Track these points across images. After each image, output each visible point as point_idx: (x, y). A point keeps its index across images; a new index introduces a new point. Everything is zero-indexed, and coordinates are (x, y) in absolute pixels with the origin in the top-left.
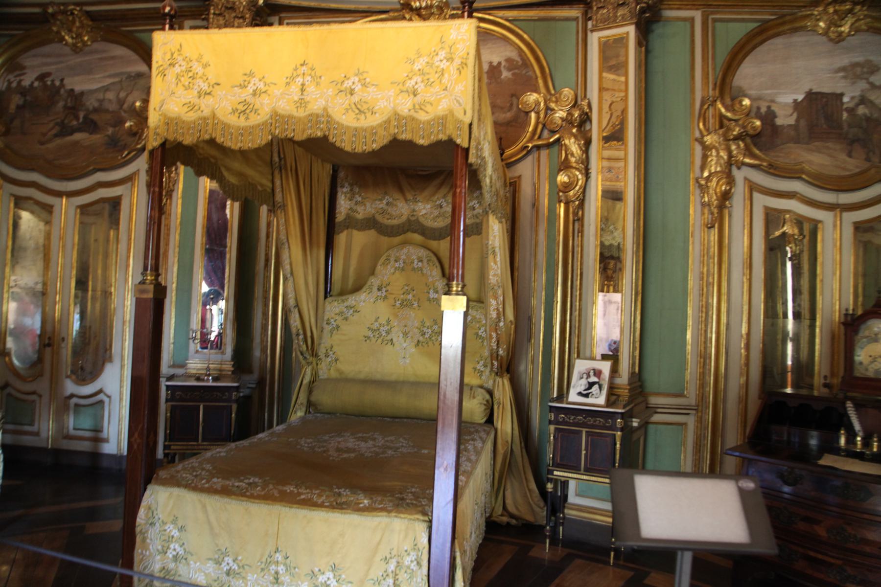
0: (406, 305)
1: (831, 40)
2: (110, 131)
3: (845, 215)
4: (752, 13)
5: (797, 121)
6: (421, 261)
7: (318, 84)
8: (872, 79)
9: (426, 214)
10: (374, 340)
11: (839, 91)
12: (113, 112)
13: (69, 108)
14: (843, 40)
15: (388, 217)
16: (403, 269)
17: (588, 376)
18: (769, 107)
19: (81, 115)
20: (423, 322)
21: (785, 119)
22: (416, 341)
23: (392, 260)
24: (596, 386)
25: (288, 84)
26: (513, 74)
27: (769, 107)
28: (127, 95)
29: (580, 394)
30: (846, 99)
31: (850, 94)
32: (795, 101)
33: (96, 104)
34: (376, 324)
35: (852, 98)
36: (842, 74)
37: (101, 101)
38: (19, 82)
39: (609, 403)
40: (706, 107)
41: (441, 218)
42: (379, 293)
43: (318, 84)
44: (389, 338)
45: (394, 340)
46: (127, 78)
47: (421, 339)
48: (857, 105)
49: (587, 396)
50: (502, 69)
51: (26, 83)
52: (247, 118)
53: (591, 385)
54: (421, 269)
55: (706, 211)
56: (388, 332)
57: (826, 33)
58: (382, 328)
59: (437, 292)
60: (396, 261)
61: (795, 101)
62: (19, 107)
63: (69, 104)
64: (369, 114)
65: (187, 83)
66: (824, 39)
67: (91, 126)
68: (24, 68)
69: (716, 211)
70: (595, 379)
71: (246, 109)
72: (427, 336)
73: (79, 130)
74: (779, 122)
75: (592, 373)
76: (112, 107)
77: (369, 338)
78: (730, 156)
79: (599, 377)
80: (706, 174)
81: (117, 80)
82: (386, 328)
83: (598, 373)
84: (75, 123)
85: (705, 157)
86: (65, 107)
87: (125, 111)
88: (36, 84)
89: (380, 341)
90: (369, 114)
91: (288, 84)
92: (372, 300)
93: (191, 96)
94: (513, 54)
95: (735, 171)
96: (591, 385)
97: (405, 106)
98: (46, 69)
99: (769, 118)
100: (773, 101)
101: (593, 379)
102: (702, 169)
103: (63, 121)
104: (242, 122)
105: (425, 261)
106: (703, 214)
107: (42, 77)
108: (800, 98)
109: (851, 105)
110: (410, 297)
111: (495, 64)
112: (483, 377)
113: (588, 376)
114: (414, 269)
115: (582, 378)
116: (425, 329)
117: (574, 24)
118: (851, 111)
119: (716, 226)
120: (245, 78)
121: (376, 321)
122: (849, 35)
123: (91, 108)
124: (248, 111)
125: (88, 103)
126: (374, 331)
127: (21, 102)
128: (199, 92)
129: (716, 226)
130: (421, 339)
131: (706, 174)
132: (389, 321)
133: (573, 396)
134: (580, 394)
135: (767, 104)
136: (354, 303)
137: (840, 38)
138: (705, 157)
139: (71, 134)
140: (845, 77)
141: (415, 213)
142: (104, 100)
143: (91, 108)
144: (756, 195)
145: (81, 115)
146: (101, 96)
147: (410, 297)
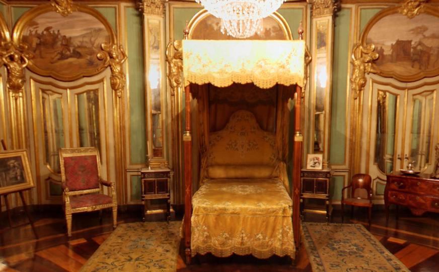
1: (408, 17)
2: (89, 57)
3: (410, 91)
5: (392, 53)
11: (410, 40)
12: (88, 48)
13: (64, 45)
14: (414, 17)
17: (314, 160)
18: (381, 48)
19: (72, 49)
21: (388, 52)
26: (276, 34)
27: (381, 48)
28: (95, 40)
29: (311, 166)
30: (413, 43)
31: (415, 40)
32: (392, 45)
33: (79, 44)
35: (416, 42)
36: (412, 32)
37: (82, 42)
38: (36, 31)
40: (355, 48)
44: (236, 147)
46: (94, 31)
48: (418, 45)
49: (314, 167)
50: (271, 32)
51: (40, 32)
53: (315, 163)
55: (353, 92)
56: (235, 146)
57: (406, 14)
60: (238, 117)
61: (392, 45)
62: (37, 45)
63: (64, 43)
66: (406, 17)
67: (77, 55)
68: (37, 24)
69: (358, 92)
70: (317, 161)
73: (71, 57)
74: (385, 53)
76: (89, 45)
78: (365, 69)
80: (354, 77)
81: (89, 31)
84: (68, 53)
85: (354, 70)
86: (62, 45)
87: (95, 48)
88: (45, 33)
94: (275, 25)
95: (366, 75)
98: (50, 25)
99: (381, 52)
100: (383, 45)
102: (352, 75)
103: (62, 52)
106: (352, 93)
107: (48, 29)
108: (394, 43)
109: (415, 46)
111: (268, 29)
117: (301, 11)
118: (415, 48)
119: (358, 98)
122: (416, 15)
123: (76, 46)
125: (74, 43)
127: (38, 42)
129: (358, 98)
130: (249, 147)
131: (354, 77)
134: (311, 166)
135: (380, 46)
137: (412, 16)
138: (354, 70)
139: (67, 58)
140: (413, 33)
142: (83, 42)
143: (76, 46)
144: (375, 84)
145: (72, 49)
146: (81, 39)
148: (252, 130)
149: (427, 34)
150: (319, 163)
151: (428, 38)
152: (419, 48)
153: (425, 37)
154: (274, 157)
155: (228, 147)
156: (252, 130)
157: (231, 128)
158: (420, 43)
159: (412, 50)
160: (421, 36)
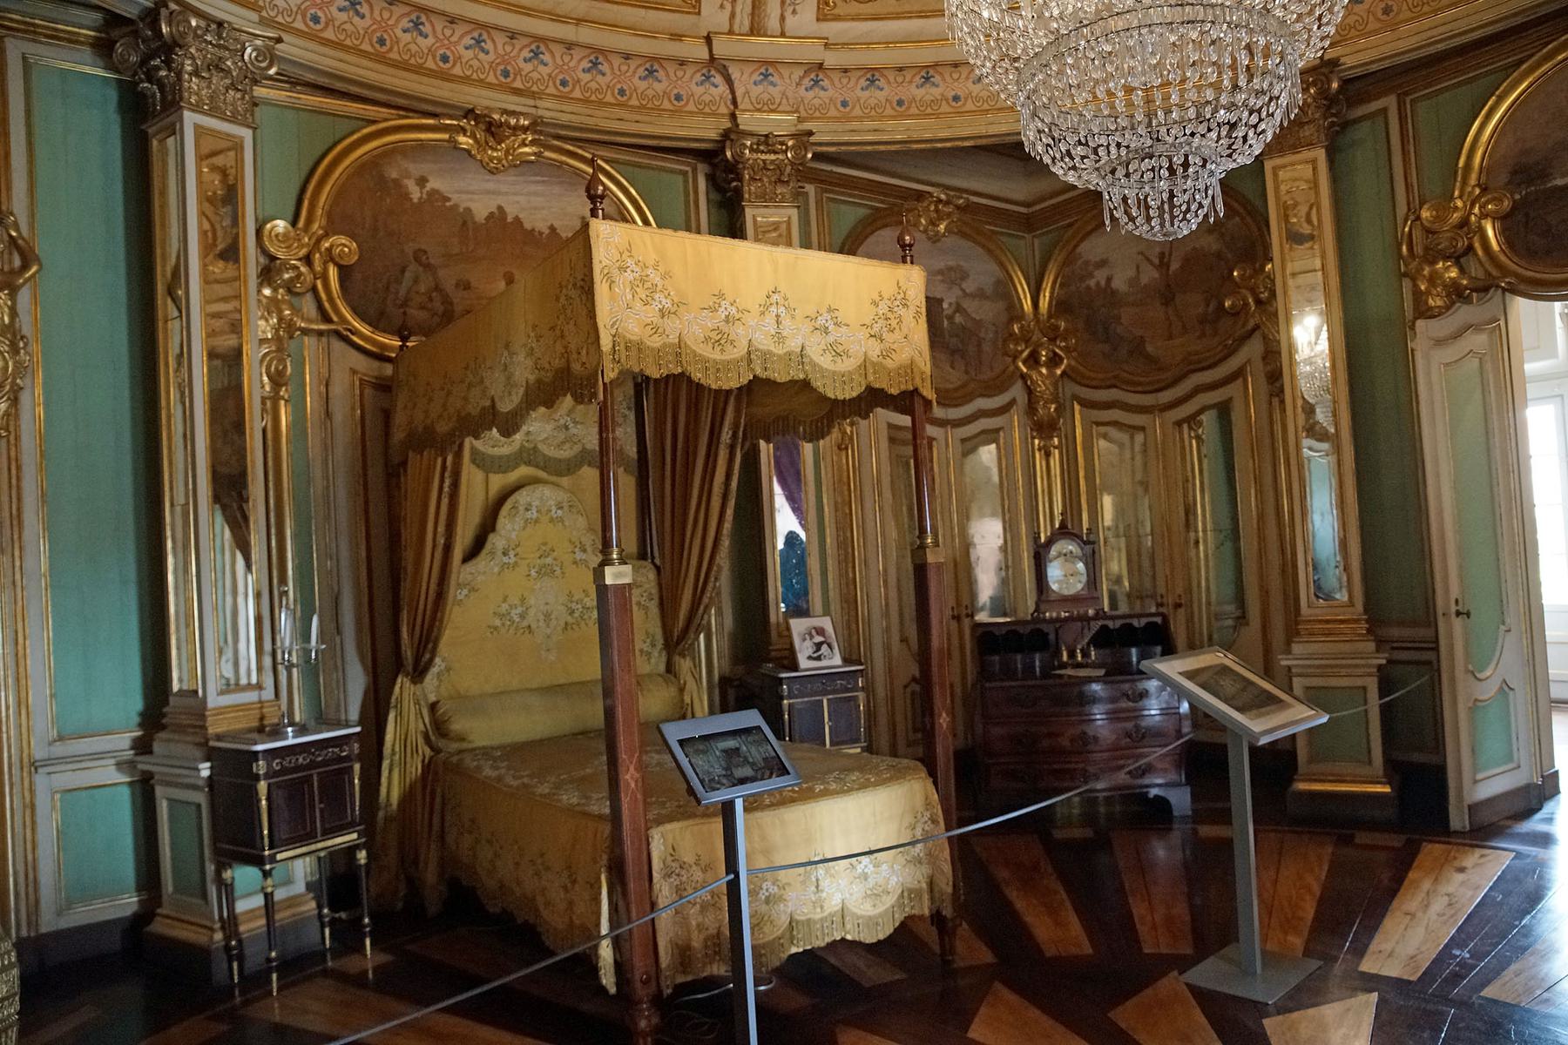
0: (545, 574)
4: (862, 198)
6: (561, 508)
7: (793, 317)
8: (964, 285)
9: (547, 439)
10: (503, 631)
14: (939, 240)
15: (491, 443)
16: (537, 521)
17: (812, 637)
20: (570, 595)
22: (563, 625)
23: (521, 508)
24: (825, 647)
25: (763, 313)
30: (945, 306)
34: (505, 607)
35: (950, 304)
36: (940, 277)
39: (847, 661)
41: (567, 446)
42: (505, 560)
43: (793, 317)
44: (525, 624)
45: (534, 626)
47: (570, 619)
48: (955, 312)
49: (819, 658)
52: (722, 351)
53: (818, 646)
54: (561, 520)
58: (513, 612)
59: (584, 551)
60: (527, 510)
64: (844, 358)
65: (644, 297)
66: (924, 236)
71: (720, 339)
72: (576, 615)
75: (814, 632)
77: (496, 628)
79: (824, 636)
82: (519, 610)
83: (820, 631)
89: (512, 631)
90: (844, 358)
91: (763, 313)
92: (496, 570)
93: (651, 313)
96: (818, 646)
97: (874, 350)
101: (819, 639)
104: (716, 355)
105: (566, 508)
109: (949, 312)
110: (549, 560)
112: (653, 661)
113: (812, 637)
114: (552, 520)
115: (804, 640)
116: (574, 606)
118: (950, 318)
120: (715, 299)
121: (505, 600)
124: (722, 342)
126: (502, 616)
128: (660, 310)
130: (570, 619)
132: (523, 600)
133: (804, 663)
136: (469, 577)
140: (943, 281)
141: (531, 438)
147: (549, 560)
148: (579, 555)
149: (970, 286)
150: (830, 646)
151: (972, 296)
152: (958, 319)
153: (965, 294)
154: (653, 645)
155: (498, 622)
156: (579, 555)
157: (505, 554)
158: (959, 308)
159: (946, 323)
160: (957, 291)
